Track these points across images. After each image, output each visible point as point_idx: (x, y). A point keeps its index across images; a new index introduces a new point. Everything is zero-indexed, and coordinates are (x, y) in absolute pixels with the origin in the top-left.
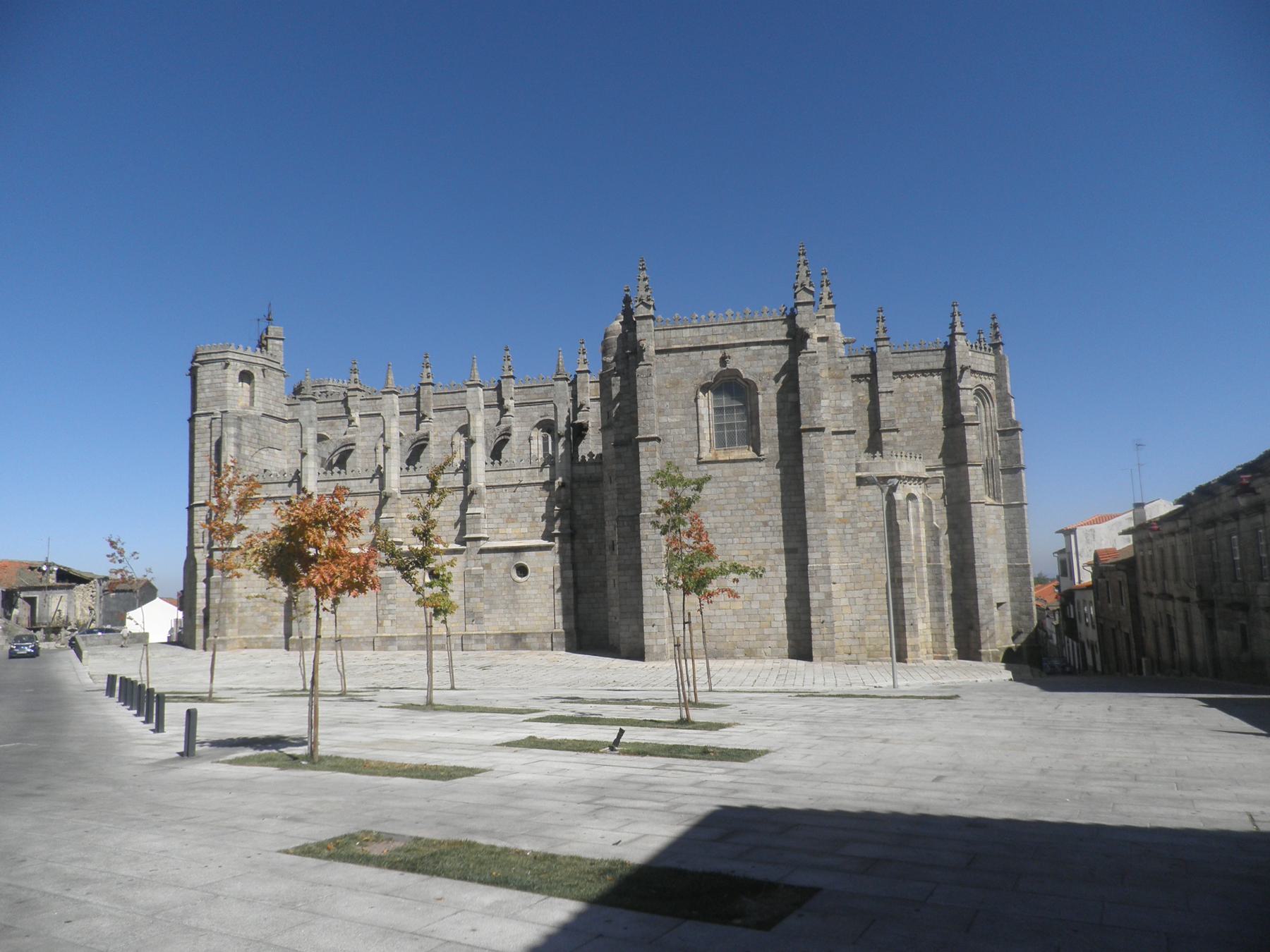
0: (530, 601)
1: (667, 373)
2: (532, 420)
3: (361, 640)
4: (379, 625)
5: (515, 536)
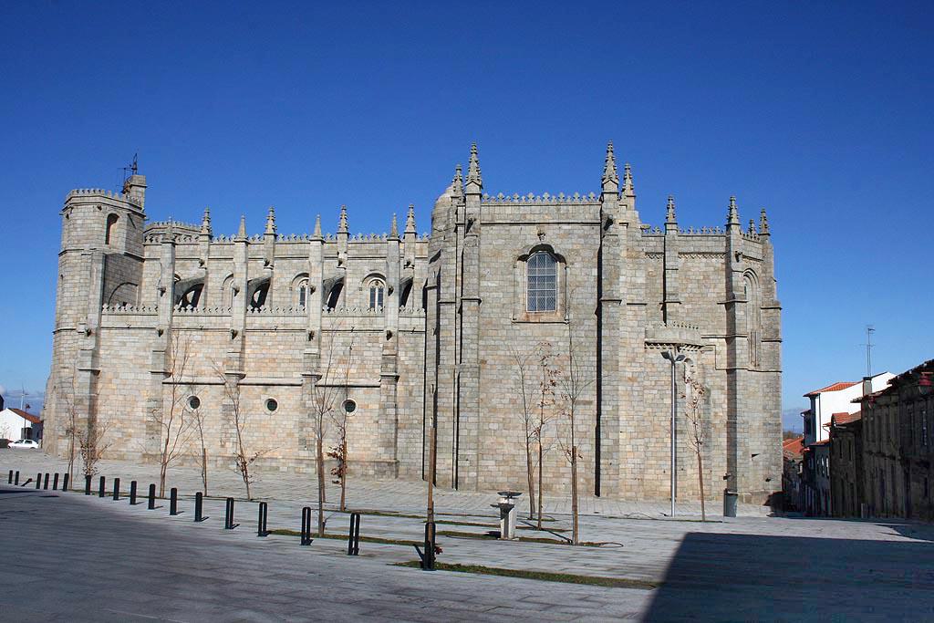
0: (356, 433)
1: (490, 244)
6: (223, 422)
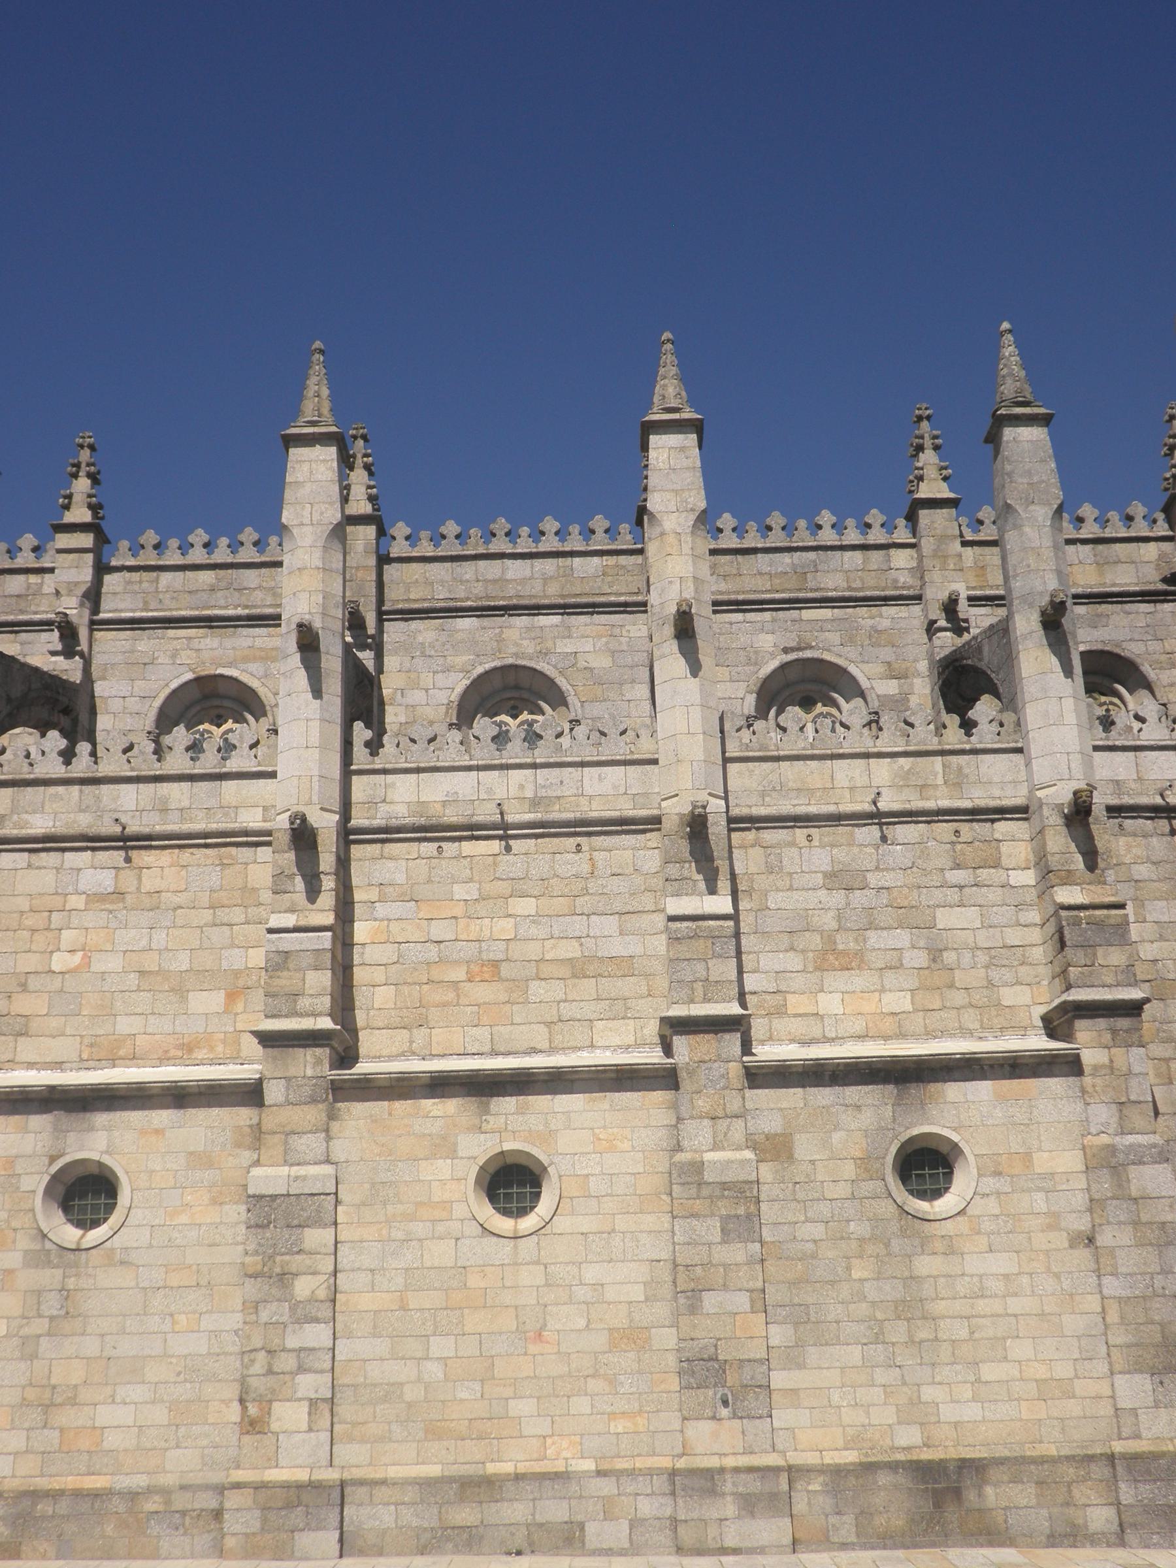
0: (982, 1305)
2: (754, 661)
3: (152, 1505)
4: (253, 1426)
5: (858, 1026)
6: (252, 1289)
